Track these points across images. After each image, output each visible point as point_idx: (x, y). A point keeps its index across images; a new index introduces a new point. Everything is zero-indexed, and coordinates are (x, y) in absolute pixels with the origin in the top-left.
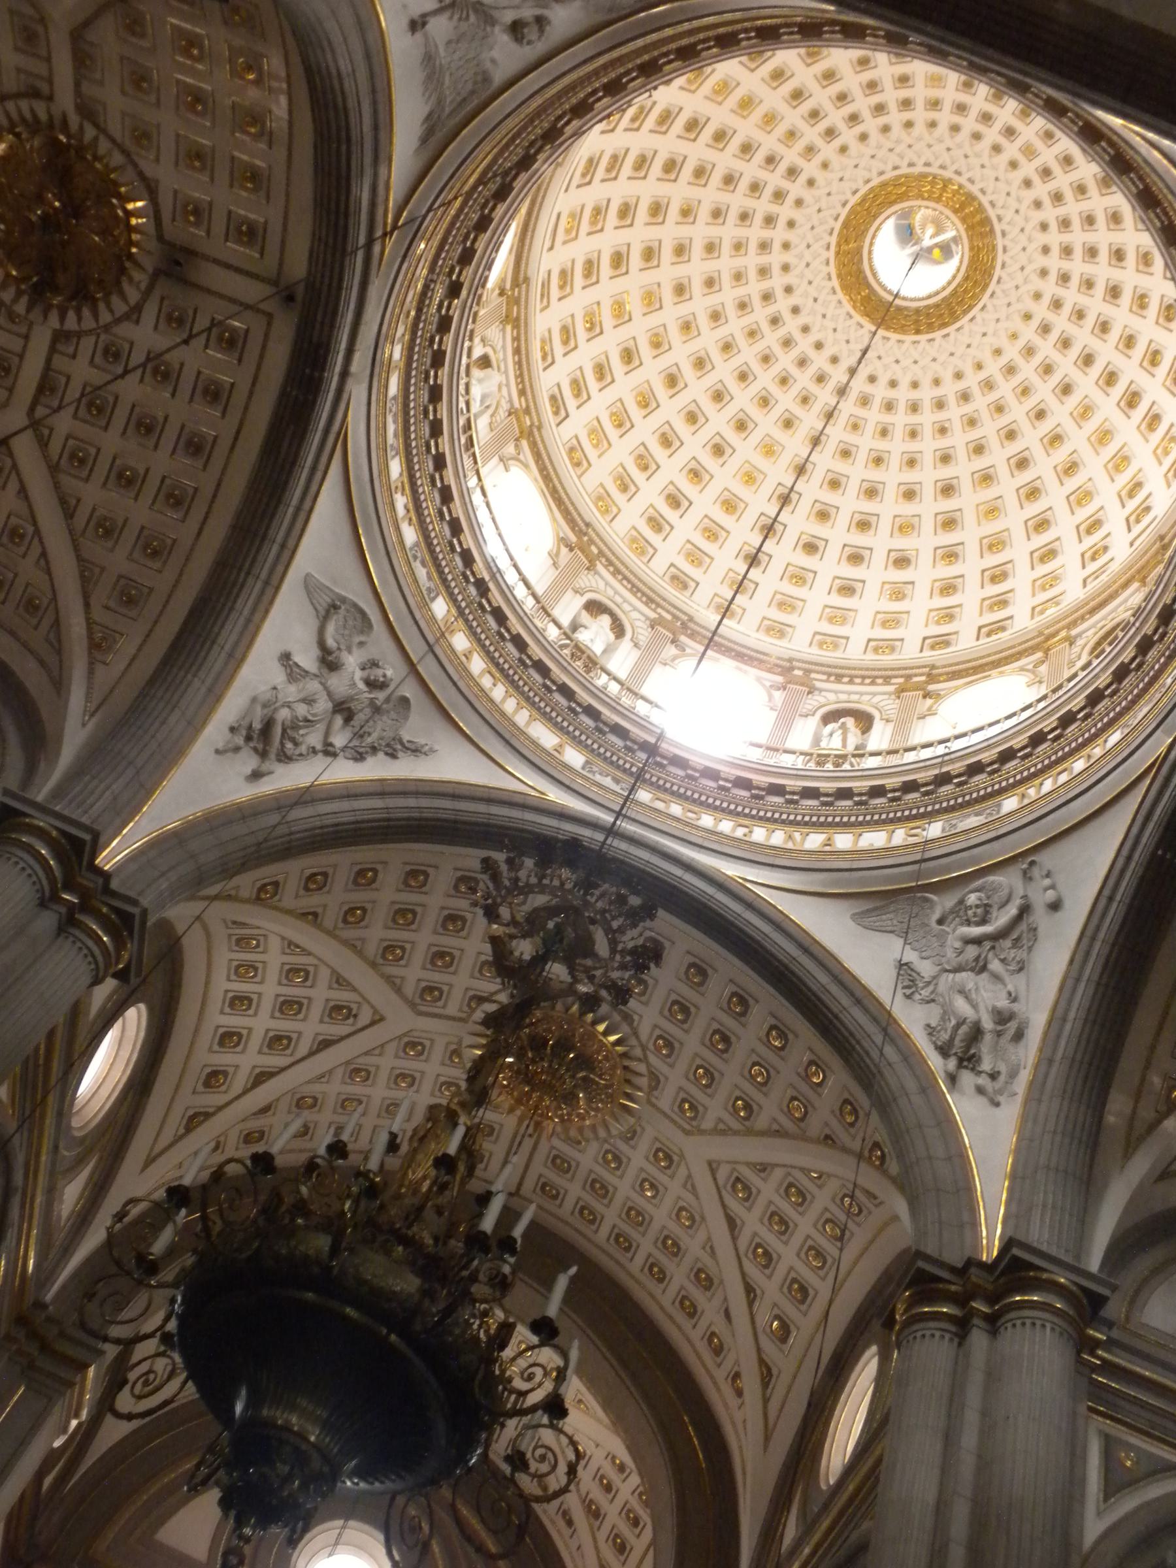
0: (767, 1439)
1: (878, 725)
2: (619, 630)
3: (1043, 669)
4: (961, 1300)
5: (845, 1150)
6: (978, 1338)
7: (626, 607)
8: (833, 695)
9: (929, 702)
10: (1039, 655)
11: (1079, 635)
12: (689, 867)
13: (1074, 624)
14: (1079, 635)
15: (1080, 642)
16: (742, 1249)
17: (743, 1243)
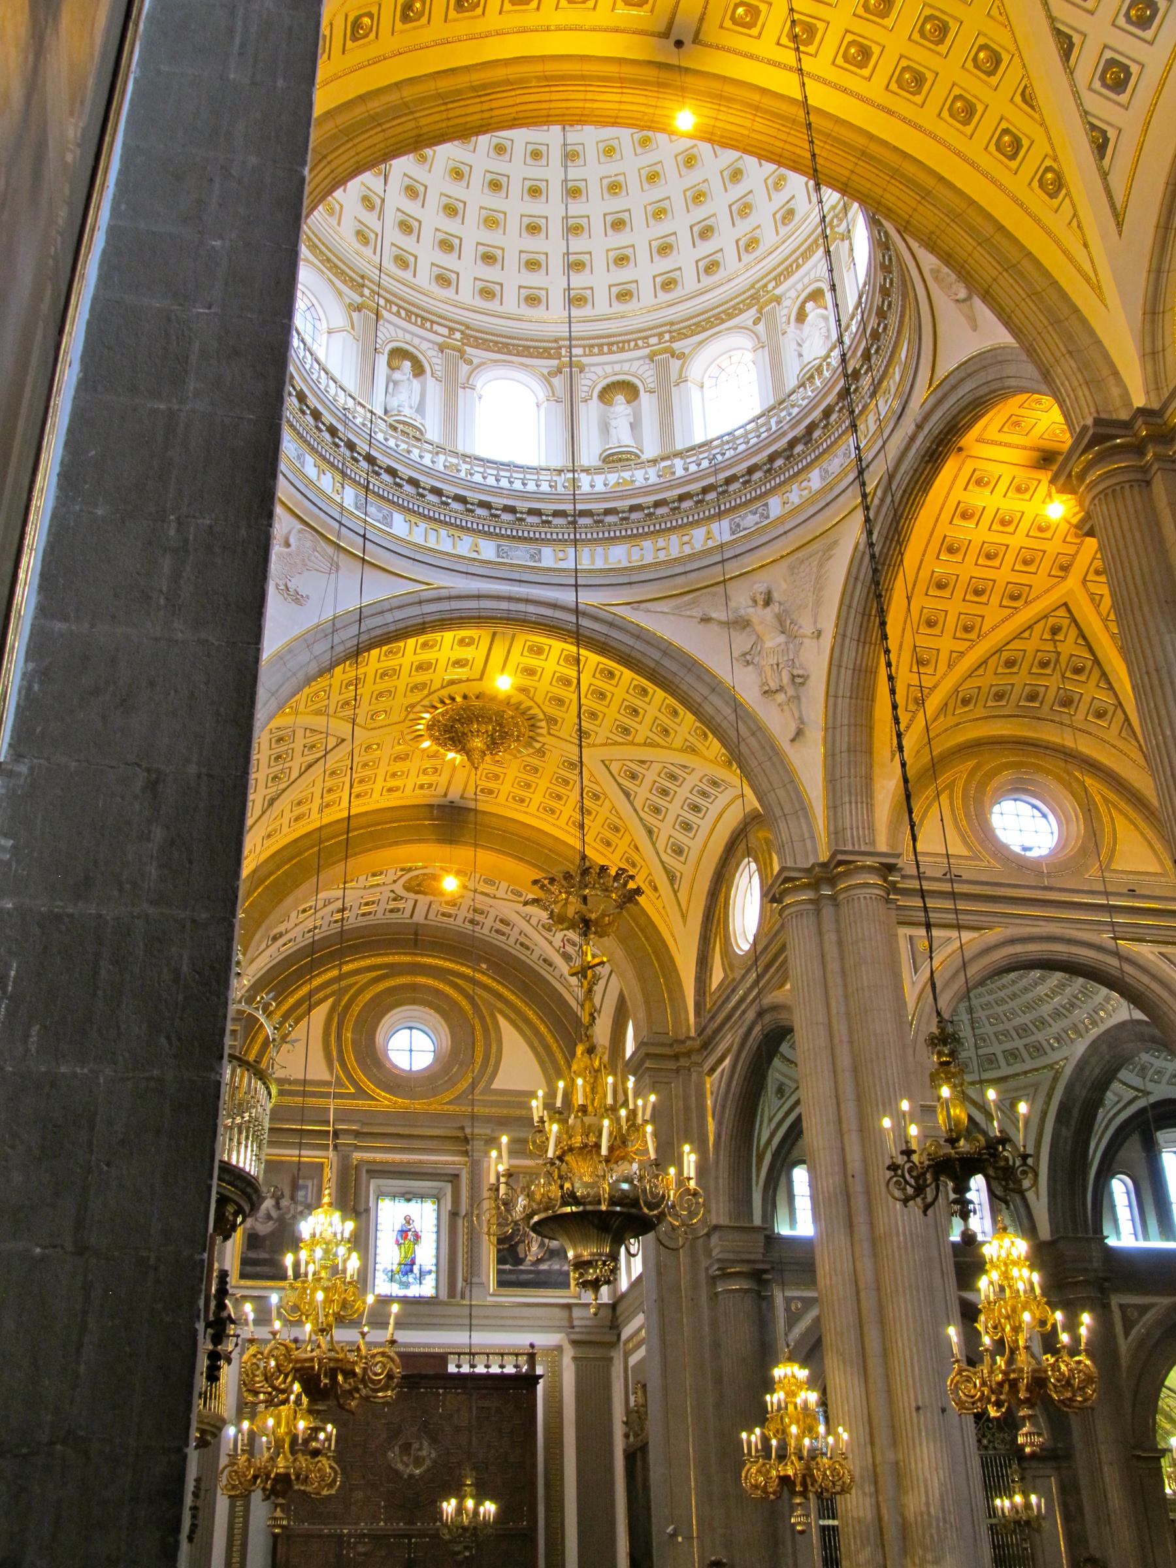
0: (684, 916)
1: (644, 397)
2: (418, 370)
3: (761, 328)
4: (815, 886)
5: (706, 759)
6: (828, 911)
7: (416, 341)
8: (600, 370)
9: (678, 363)
10: (753, 311)
11: (784, 294)
12: (554, 606)
13: (778, 281)
14: (784, 294)
15: (787, 303)
16: (639, 807)
17: (638, 804)
